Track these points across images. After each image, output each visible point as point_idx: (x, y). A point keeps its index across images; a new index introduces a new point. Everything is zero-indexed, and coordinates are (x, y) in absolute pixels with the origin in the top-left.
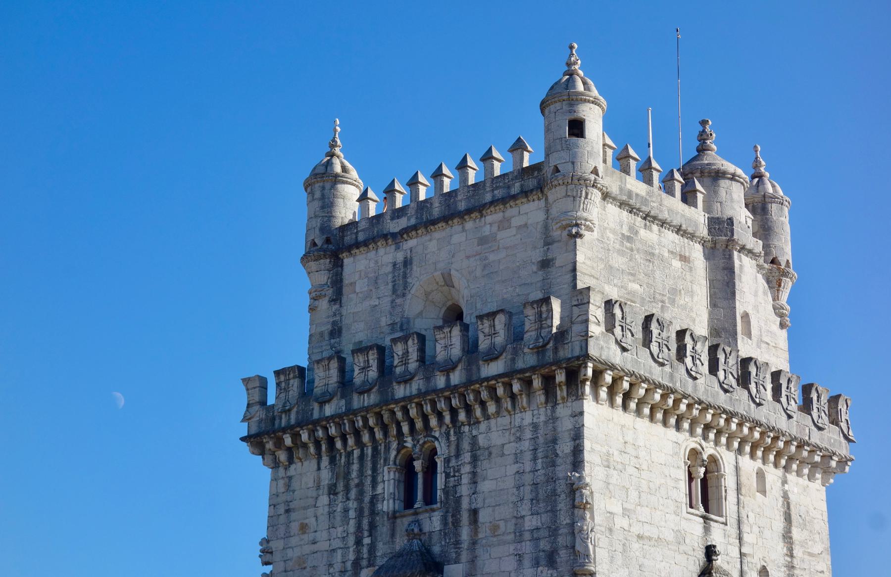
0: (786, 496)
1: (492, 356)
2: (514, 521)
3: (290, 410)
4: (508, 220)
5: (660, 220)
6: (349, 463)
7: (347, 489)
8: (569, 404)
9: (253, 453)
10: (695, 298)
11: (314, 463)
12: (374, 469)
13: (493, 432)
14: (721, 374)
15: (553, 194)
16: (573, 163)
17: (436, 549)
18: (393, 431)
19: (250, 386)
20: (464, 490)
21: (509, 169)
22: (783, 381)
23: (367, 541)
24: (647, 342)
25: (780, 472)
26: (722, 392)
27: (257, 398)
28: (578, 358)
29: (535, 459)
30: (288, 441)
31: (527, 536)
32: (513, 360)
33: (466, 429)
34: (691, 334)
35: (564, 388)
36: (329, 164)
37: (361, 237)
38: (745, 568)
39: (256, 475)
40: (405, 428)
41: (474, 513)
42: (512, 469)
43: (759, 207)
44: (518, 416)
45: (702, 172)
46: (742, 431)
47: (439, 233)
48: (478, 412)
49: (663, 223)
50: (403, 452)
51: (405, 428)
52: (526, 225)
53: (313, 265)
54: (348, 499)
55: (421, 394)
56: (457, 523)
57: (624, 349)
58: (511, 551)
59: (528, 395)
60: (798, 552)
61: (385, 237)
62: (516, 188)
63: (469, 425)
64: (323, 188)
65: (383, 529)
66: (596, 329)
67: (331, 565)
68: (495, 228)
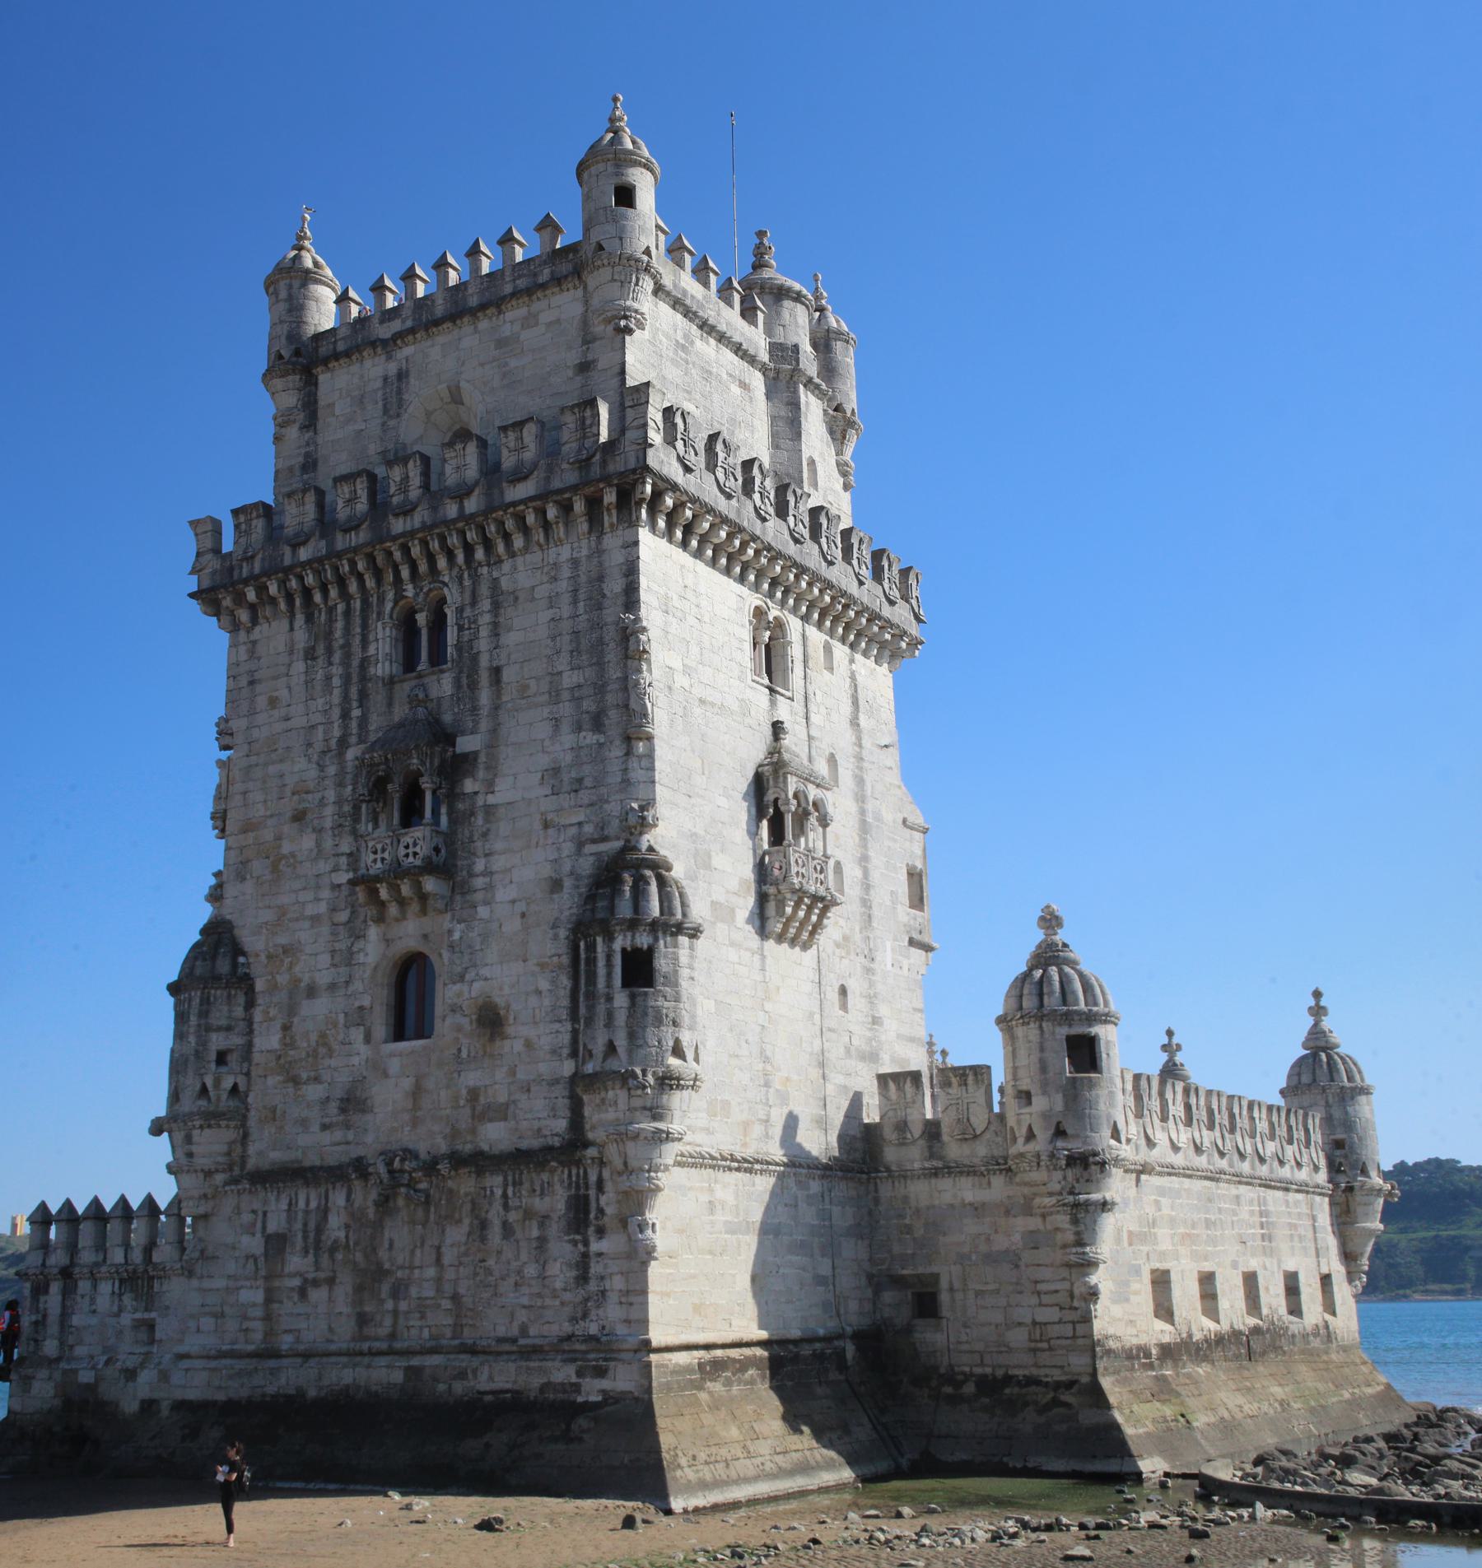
0: (853, 677)
1: (519, 476)
2: (548, 678)
3: (253, 557)
4: (535, 316)
6: (331, 620)
7: (329, 651)
8: (619, 533)
9: (205, 613)
11: (285, 624)
12: (365, 626)
13: (521, 572)
15: (592, 280)
17: (447, 718)
18: (389, 577)
19: (199, 530)
20: (483, 644)
21: (536, 252)
22: (855, 541)
23: (356, 713)
24: (711, 466)
25: (847, 649)
27: (209, 544)
28: (634, 471)
29: (575, 602)
30: (251, 595)
31: (566, 695)
32: (548, 479)
33: (485, 570)
35: (614, 512)
36: (297, 258)
37: (341, 347)
38: (813, 753)
39: (209, 643)
40: (405, 573)
41: (496, 672)
42: (549, 614)
43: (823, 342)
44: (553, 551)
45: (762, 288)
46: (811, 591)
47: (444, 337)
48: (501, 548)
50: (402, 603)
51: (405, 573)
52: (558, 321)
53: (279, 383)
54: (331, 664)
55: (424, 527)
56: (473, 686)
58: (545, 715)
59: (566, 525)
60: (867, 742)
61: (373, 344)
62: (545, 274)
63: (489, 565)
64: (290, 287)
65: (378, 697)
66: (655, 437)
67: (309, 745)
68: (517, 327)
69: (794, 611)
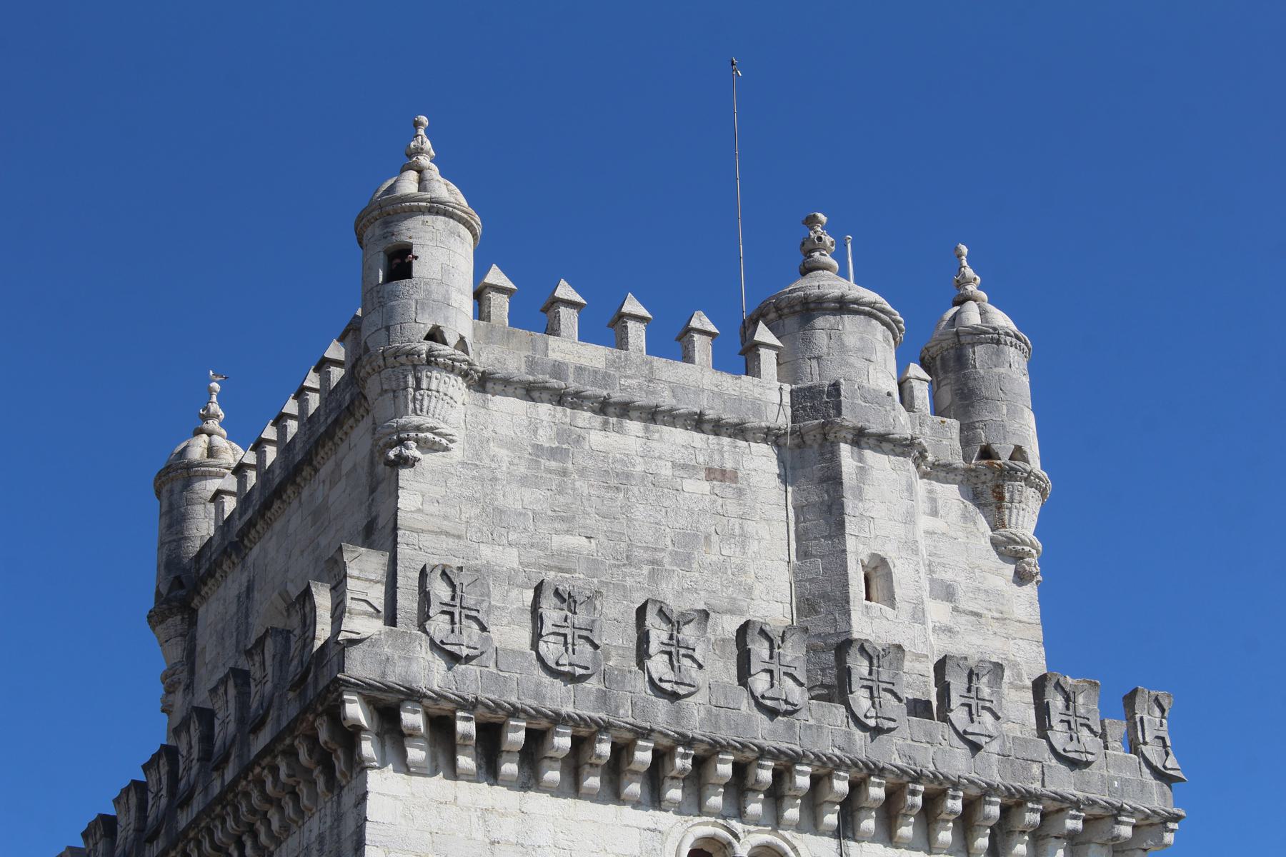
5: (641, 408)
10: (753, 547)
14: (760, 683)
16: (388, 328)
26: (762, 718)
34: (661, 611)
45: (778, 309)
49: (653, 415)
52: (354, 468)
57: (454, 659)
64: (171, 492)
69: (811, 823)
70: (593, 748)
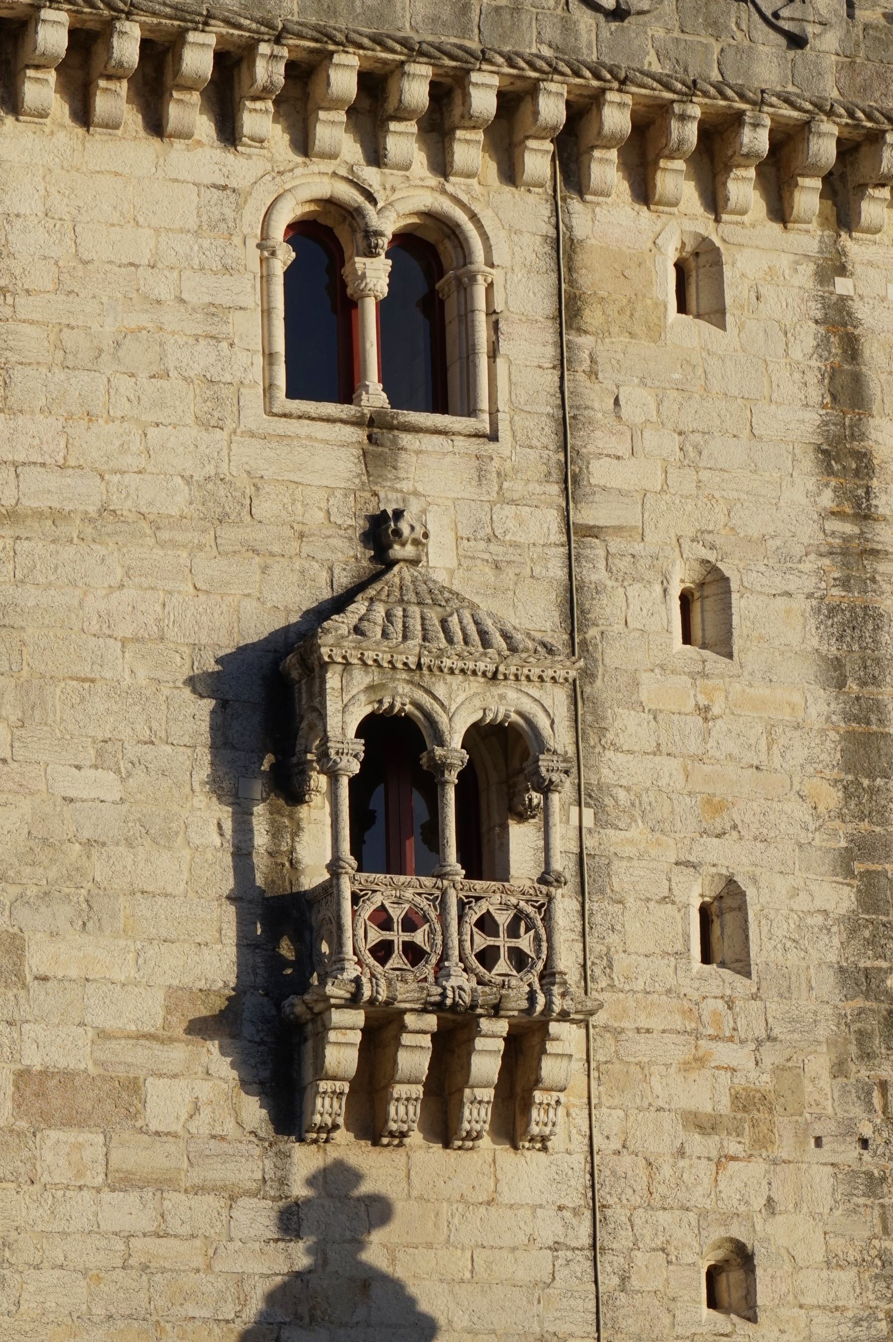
38: (594, 573)
70: (109, 48)
